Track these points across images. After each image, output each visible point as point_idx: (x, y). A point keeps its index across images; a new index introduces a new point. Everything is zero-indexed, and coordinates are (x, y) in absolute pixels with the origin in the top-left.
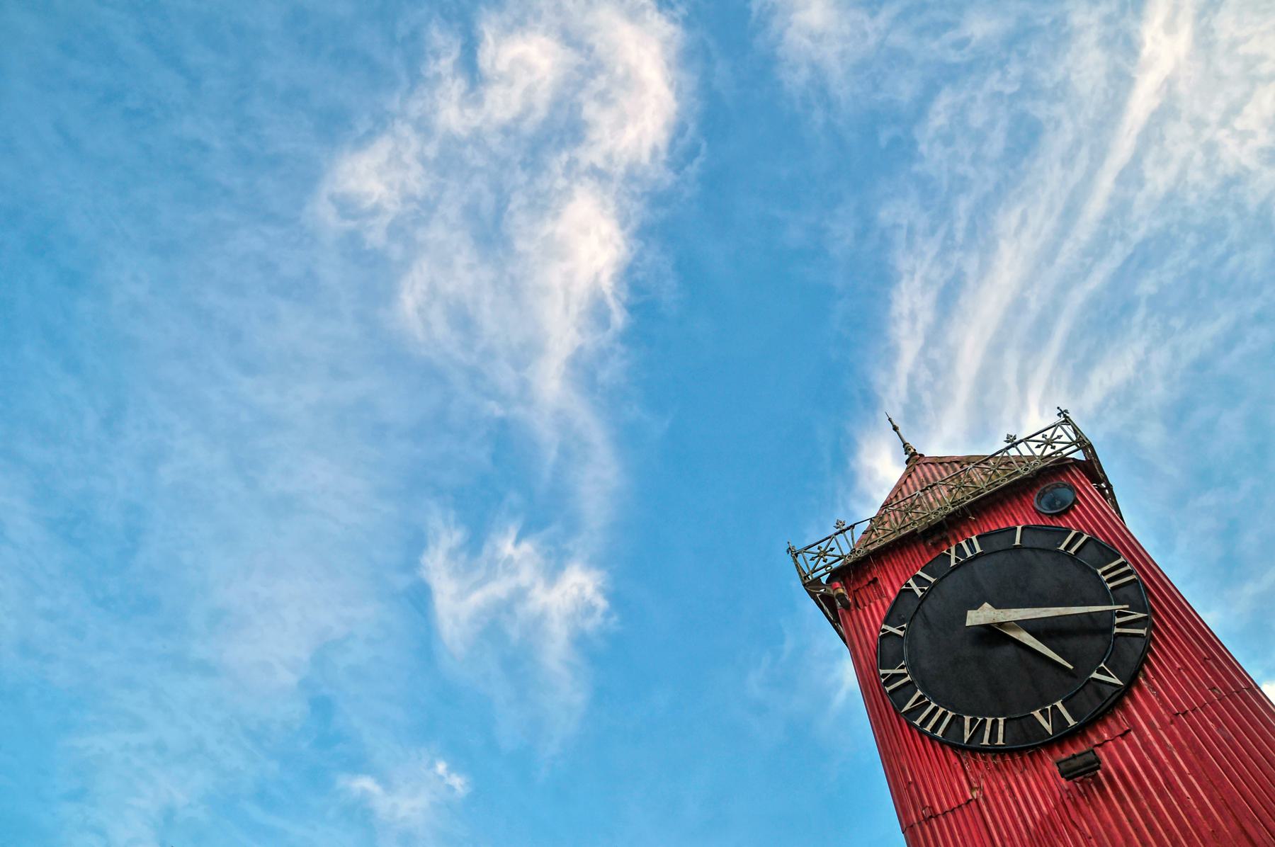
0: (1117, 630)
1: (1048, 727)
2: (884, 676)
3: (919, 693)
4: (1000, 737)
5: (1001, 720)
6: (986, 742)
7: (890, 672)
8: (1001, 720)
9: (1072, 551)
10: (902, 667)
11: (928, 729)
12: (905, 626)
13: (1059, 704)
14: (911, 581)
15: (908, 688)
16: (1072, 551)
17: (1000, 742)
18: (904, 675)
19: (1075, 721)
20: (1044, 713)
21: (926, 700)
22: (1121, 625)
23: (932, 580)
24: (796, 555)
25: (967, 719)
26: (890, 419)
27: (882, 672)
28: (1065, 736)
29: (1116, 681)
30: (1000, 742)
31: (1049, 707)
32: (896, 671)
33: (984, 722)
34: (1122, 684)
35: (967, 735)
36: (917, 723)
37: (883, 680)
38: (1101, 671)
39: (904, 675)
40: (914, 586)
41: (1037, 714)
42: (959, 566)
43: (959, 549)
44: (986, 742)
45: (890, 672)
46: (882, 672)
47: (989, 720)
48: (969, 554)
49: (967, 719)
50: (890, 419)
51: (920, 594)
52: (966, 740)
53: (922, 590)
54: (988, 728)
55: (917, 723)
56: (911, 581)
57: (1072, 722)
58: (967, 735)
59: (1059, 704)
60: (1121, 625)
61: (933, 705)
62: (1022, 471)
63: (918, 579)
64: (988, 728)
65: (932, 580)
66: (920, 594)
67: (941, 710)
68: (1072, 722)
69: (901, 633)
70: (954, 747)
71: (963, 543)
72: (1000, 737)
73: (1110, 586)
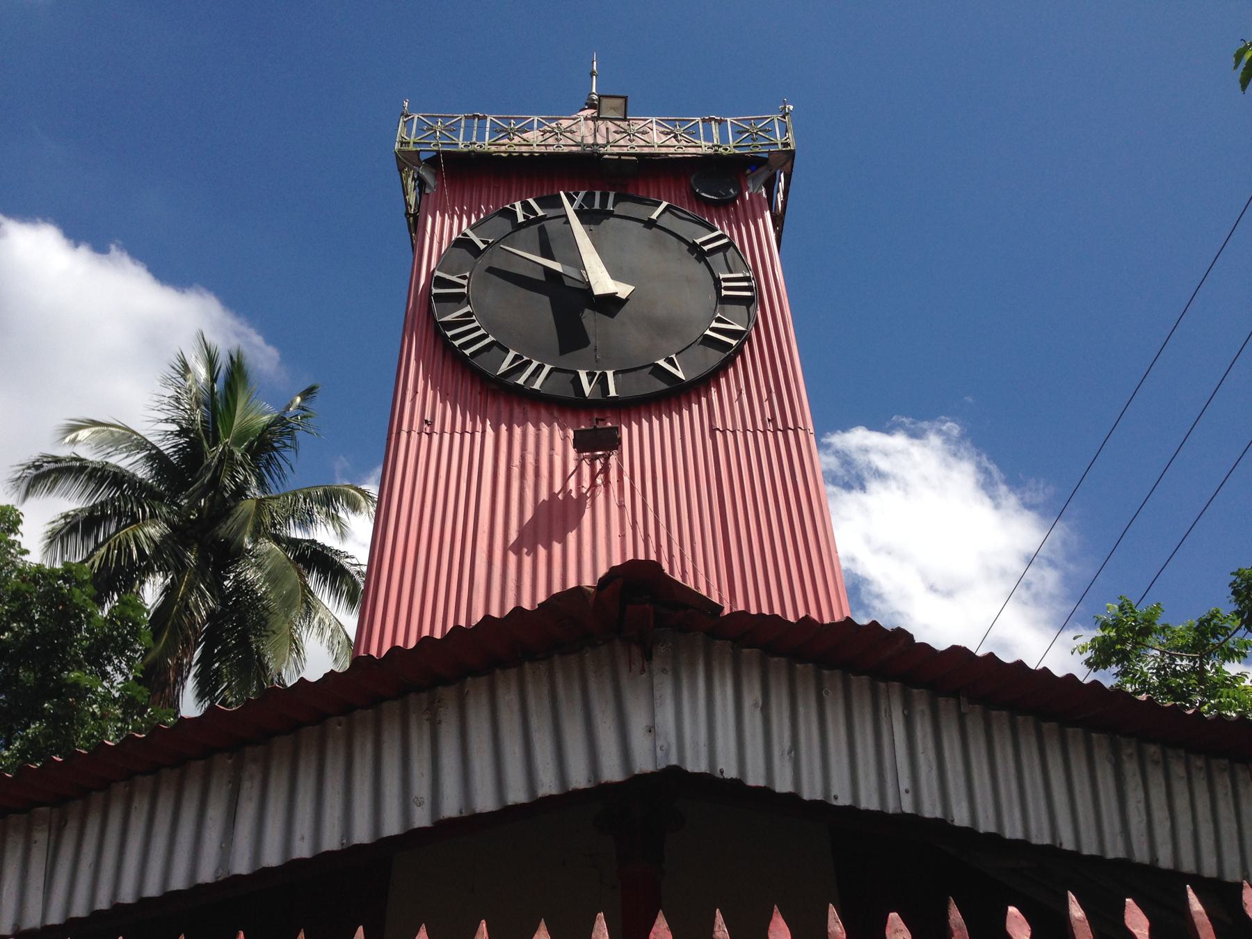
0: (708, 332)
3: (468, 309)
9: (706, 248)
10: (464, 278)
13: (610, 374)
19: (617, 393)
20: (591, 375)
21: (474, 318)
22: (714, 330)
28: (603, 405)
29: (680, 375)
31: (598, 372)
32: (454, 279)
38: (671, 362)
39: (462, 286)
48: (597, 206)
51: (521, 219)
53: (525, 217)
59: (610, 374)
63: (526, 207)
66: (521, 219)
67: (482, 331)
71: (598, 194)
73: (724, 293)
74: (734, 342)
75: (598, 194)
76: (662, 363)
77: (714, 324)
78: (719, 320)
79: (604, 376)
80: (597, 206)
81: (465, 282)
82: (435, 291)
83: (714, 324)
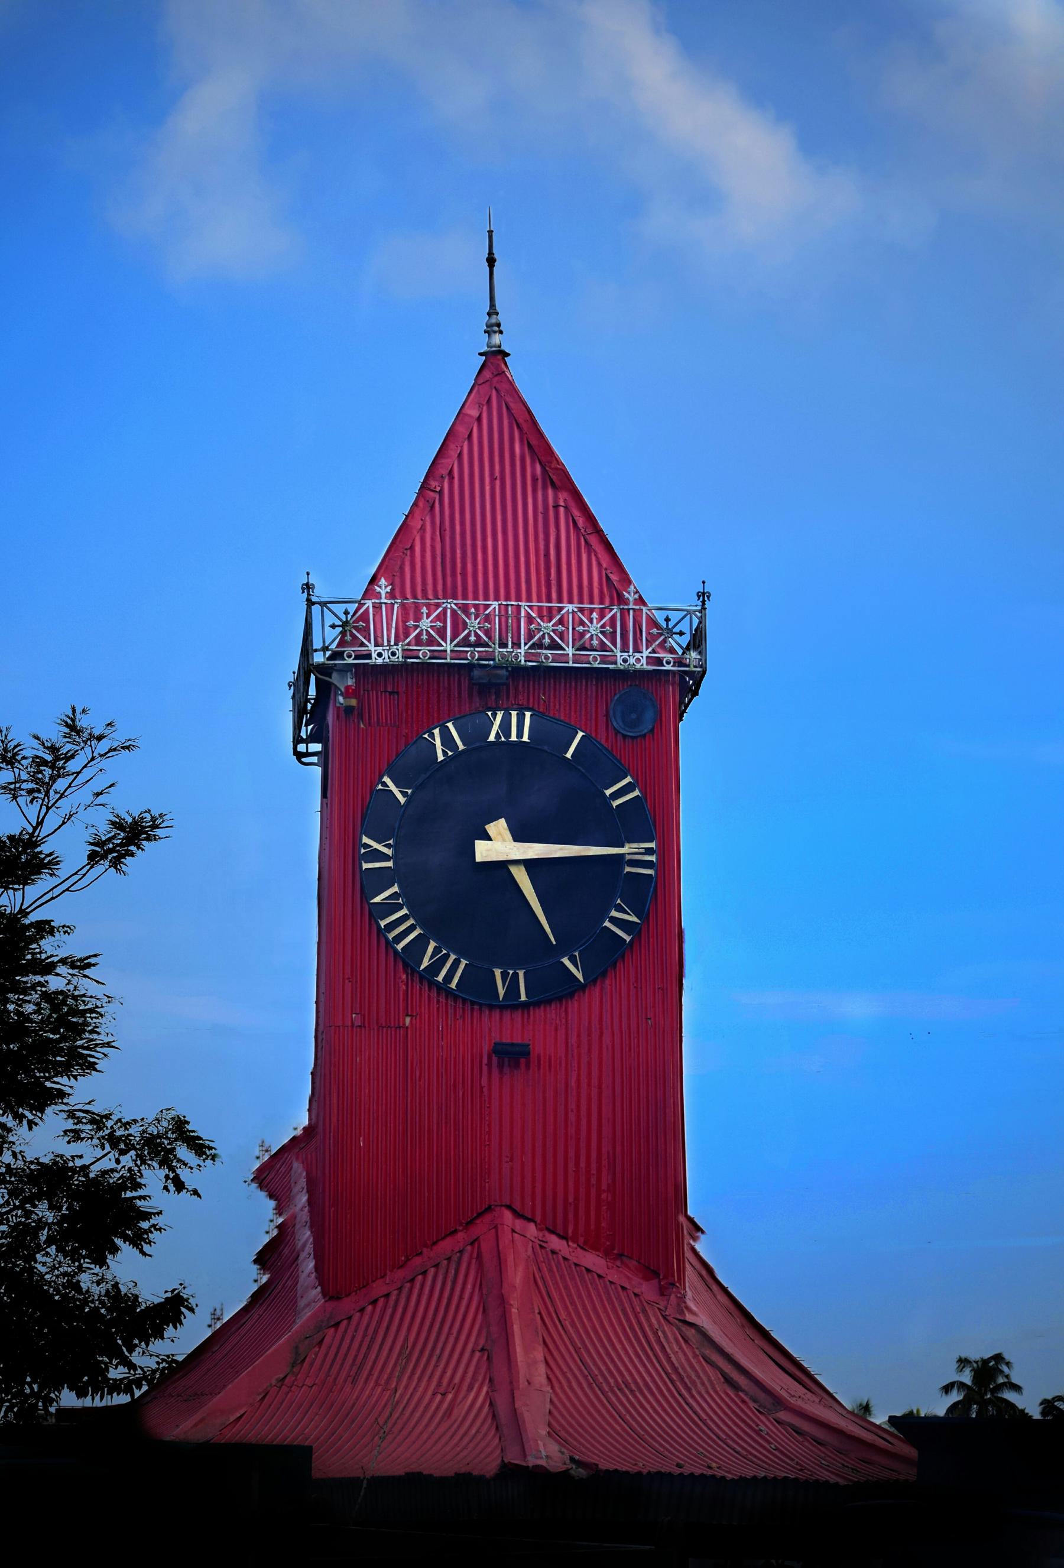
0: (607, 924)
1: (501, 992)
2: (366, 846)
3: (395, 889)
4: (456, 980)
5: (464, 962)
6: (440, 978)
7: (375, 845)
8: (464, 962)
10: (388, 846)
11: (391, 936)
12: (409, 791)
13: (521, 973)
14: (436, 732)
15: (382, 879)
16: (616, 803)
17: (453, 985)
18: (385, 857)
20: (504, 975)
22: (613, 920)
23: (461, 747)
24: (314, 603)
25: (432, 945)
26: (490, 232)
27: (365, 840)
30: (453, 985)
33: (447, 956)
34: (582, 980)
35: (426, 963)
36: (383, 923)
37: (363, 851)
38: (573, 960)
39: (385, 857)
40: (438, 742)
41: (498, 972)
42: (497, 743)
43: (505, 726)
44: (440, 978)
45: (375, 845)
46: (365, 840)
47: (453, 957)
48: (514, 738)
49: (432, 945)
50: (490, 232)
51: (441, 757)
52: (422, 967)
53: (445, 753)
54: (448, 965)
55: (383, 923)
56: (436, 732)
57: (523, 998)
58: (426, 963)
59: (521, 973)
60: (613, 920)
61: (404, 911)
62: (620, 661)
64: (448, 965)
65: (461, 747)
68: (523, 998)
69: (402, 800)
70: (406, 965)
71: (514, 714)
72: (456, 980)
74: (628, 938)
75: (514, 714)
76: (566, 961)
77: (614, 913)
78: (620, 909)
79: (516, 975)
80: (514, 738)
81: (389, 852)
82: (365, 866)
83: (614, 913)
